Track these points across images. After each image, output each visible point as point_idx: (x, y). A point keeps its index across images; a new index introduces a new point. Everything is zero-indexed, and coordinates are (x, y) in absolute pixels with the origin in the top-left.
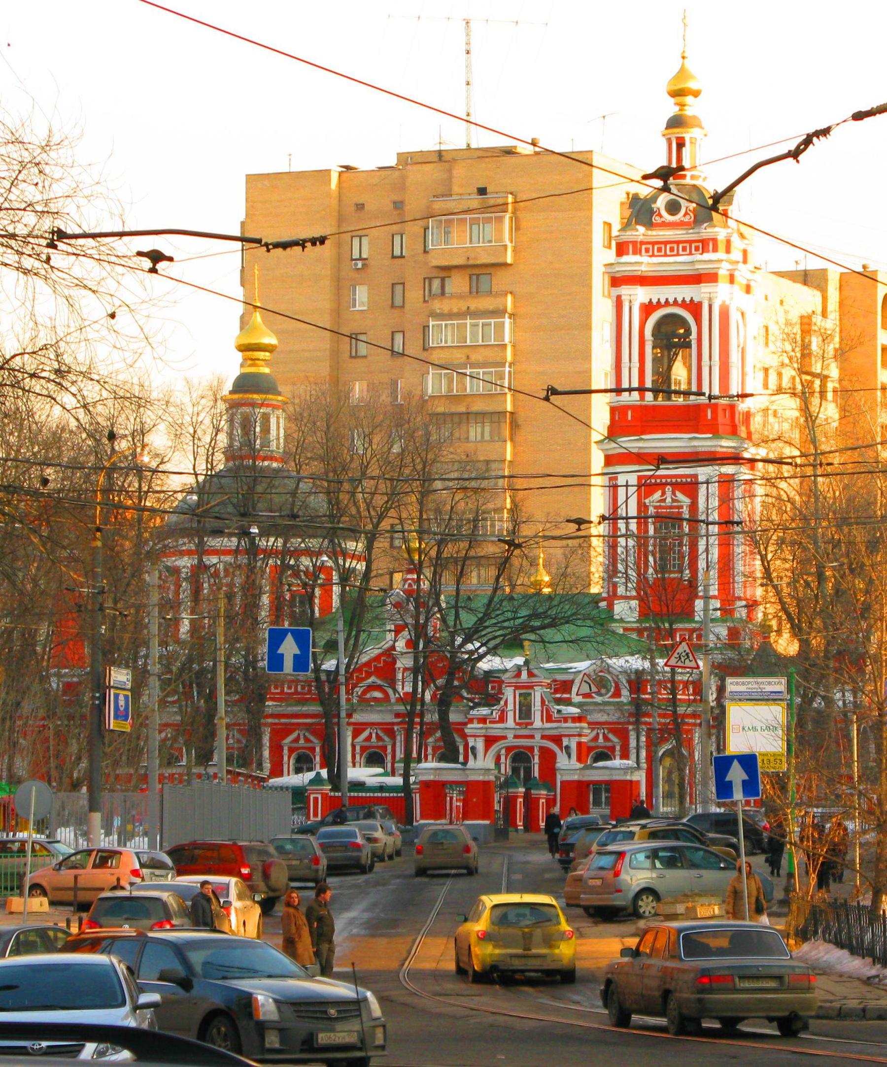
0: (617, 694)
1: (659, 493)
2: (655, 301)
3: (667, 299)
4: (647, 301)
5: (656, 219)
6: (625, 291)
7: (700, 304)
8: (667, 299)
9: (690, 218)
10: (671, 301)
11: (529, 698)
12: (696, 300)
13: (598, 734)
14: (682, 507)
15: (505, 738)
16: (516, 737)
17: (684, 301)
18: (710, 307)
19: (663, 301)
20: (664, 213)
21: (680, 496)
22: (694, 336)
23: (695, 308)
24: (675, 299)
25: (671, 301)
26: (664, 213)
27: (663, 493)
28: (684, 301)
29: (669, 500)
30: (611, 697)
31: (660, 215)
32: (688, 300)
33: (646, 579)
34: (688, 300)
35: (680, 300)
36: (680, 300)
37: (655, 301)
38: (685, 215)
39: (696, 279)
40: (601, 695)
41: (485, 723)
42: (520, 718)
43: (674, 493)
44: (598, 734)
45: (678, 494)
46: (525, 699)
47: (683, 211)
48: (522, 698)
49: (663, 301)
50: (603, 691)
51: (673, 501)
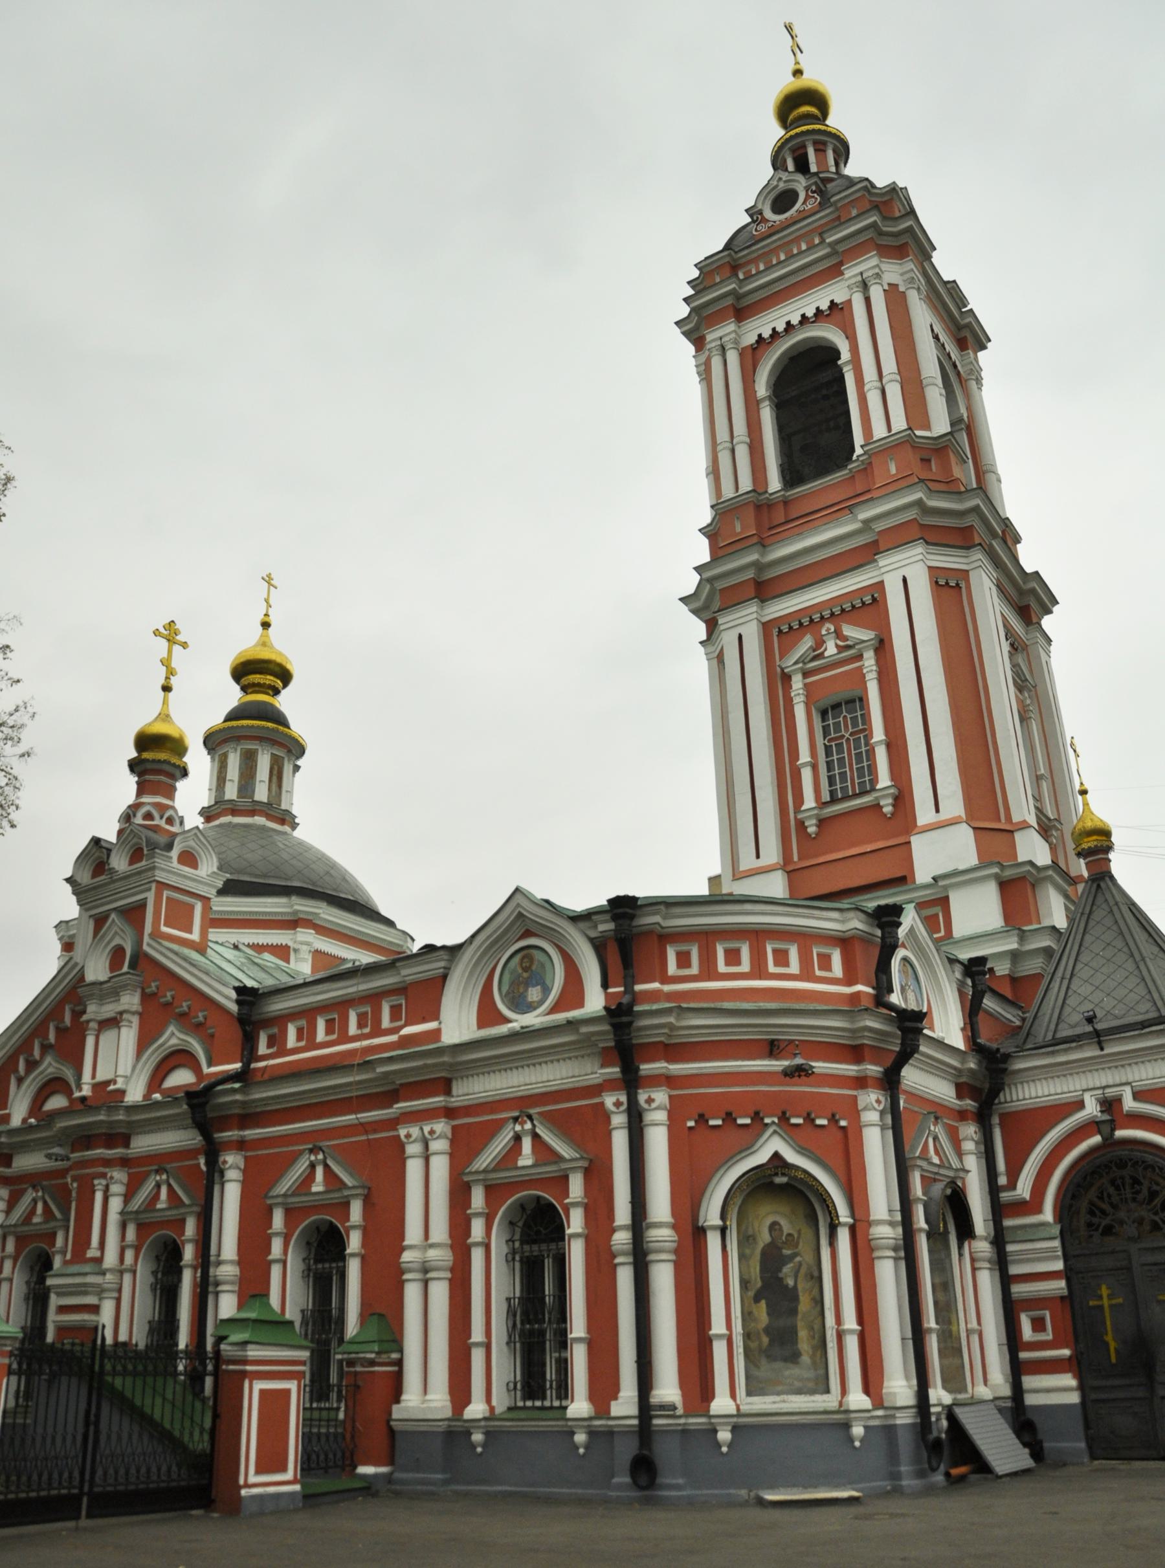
0: (573, 993)
1: (807, 642)
2: (766, 334)
4: (751, 339)
7: (849, 302)
8: (788, 323)
10: (795, 321)
12: (838, 300)
13: (518, 1138)
14: (860, 657)
18: (868, 300)
20: (768, 214)
21: (852, 632)
22: (845, 356)
23: (837, 312)
25: (795, 321)
26: (768, 214)
27: (820, 643)
28: (819, 312)
29: (831, 649)
30: (554, 1010)
31: (765, 220)
32: (824, 306)
33: (801, 825)
35: (810, 313)
36: (810, 313)
38: (804, 203)
39: (834, 272)
40: (530, 1007)
43: (838, 634)
44: (518, 1138)
45: (849, 631)
49: (781, 327)
50: (534, 994)
51: (841, 649)
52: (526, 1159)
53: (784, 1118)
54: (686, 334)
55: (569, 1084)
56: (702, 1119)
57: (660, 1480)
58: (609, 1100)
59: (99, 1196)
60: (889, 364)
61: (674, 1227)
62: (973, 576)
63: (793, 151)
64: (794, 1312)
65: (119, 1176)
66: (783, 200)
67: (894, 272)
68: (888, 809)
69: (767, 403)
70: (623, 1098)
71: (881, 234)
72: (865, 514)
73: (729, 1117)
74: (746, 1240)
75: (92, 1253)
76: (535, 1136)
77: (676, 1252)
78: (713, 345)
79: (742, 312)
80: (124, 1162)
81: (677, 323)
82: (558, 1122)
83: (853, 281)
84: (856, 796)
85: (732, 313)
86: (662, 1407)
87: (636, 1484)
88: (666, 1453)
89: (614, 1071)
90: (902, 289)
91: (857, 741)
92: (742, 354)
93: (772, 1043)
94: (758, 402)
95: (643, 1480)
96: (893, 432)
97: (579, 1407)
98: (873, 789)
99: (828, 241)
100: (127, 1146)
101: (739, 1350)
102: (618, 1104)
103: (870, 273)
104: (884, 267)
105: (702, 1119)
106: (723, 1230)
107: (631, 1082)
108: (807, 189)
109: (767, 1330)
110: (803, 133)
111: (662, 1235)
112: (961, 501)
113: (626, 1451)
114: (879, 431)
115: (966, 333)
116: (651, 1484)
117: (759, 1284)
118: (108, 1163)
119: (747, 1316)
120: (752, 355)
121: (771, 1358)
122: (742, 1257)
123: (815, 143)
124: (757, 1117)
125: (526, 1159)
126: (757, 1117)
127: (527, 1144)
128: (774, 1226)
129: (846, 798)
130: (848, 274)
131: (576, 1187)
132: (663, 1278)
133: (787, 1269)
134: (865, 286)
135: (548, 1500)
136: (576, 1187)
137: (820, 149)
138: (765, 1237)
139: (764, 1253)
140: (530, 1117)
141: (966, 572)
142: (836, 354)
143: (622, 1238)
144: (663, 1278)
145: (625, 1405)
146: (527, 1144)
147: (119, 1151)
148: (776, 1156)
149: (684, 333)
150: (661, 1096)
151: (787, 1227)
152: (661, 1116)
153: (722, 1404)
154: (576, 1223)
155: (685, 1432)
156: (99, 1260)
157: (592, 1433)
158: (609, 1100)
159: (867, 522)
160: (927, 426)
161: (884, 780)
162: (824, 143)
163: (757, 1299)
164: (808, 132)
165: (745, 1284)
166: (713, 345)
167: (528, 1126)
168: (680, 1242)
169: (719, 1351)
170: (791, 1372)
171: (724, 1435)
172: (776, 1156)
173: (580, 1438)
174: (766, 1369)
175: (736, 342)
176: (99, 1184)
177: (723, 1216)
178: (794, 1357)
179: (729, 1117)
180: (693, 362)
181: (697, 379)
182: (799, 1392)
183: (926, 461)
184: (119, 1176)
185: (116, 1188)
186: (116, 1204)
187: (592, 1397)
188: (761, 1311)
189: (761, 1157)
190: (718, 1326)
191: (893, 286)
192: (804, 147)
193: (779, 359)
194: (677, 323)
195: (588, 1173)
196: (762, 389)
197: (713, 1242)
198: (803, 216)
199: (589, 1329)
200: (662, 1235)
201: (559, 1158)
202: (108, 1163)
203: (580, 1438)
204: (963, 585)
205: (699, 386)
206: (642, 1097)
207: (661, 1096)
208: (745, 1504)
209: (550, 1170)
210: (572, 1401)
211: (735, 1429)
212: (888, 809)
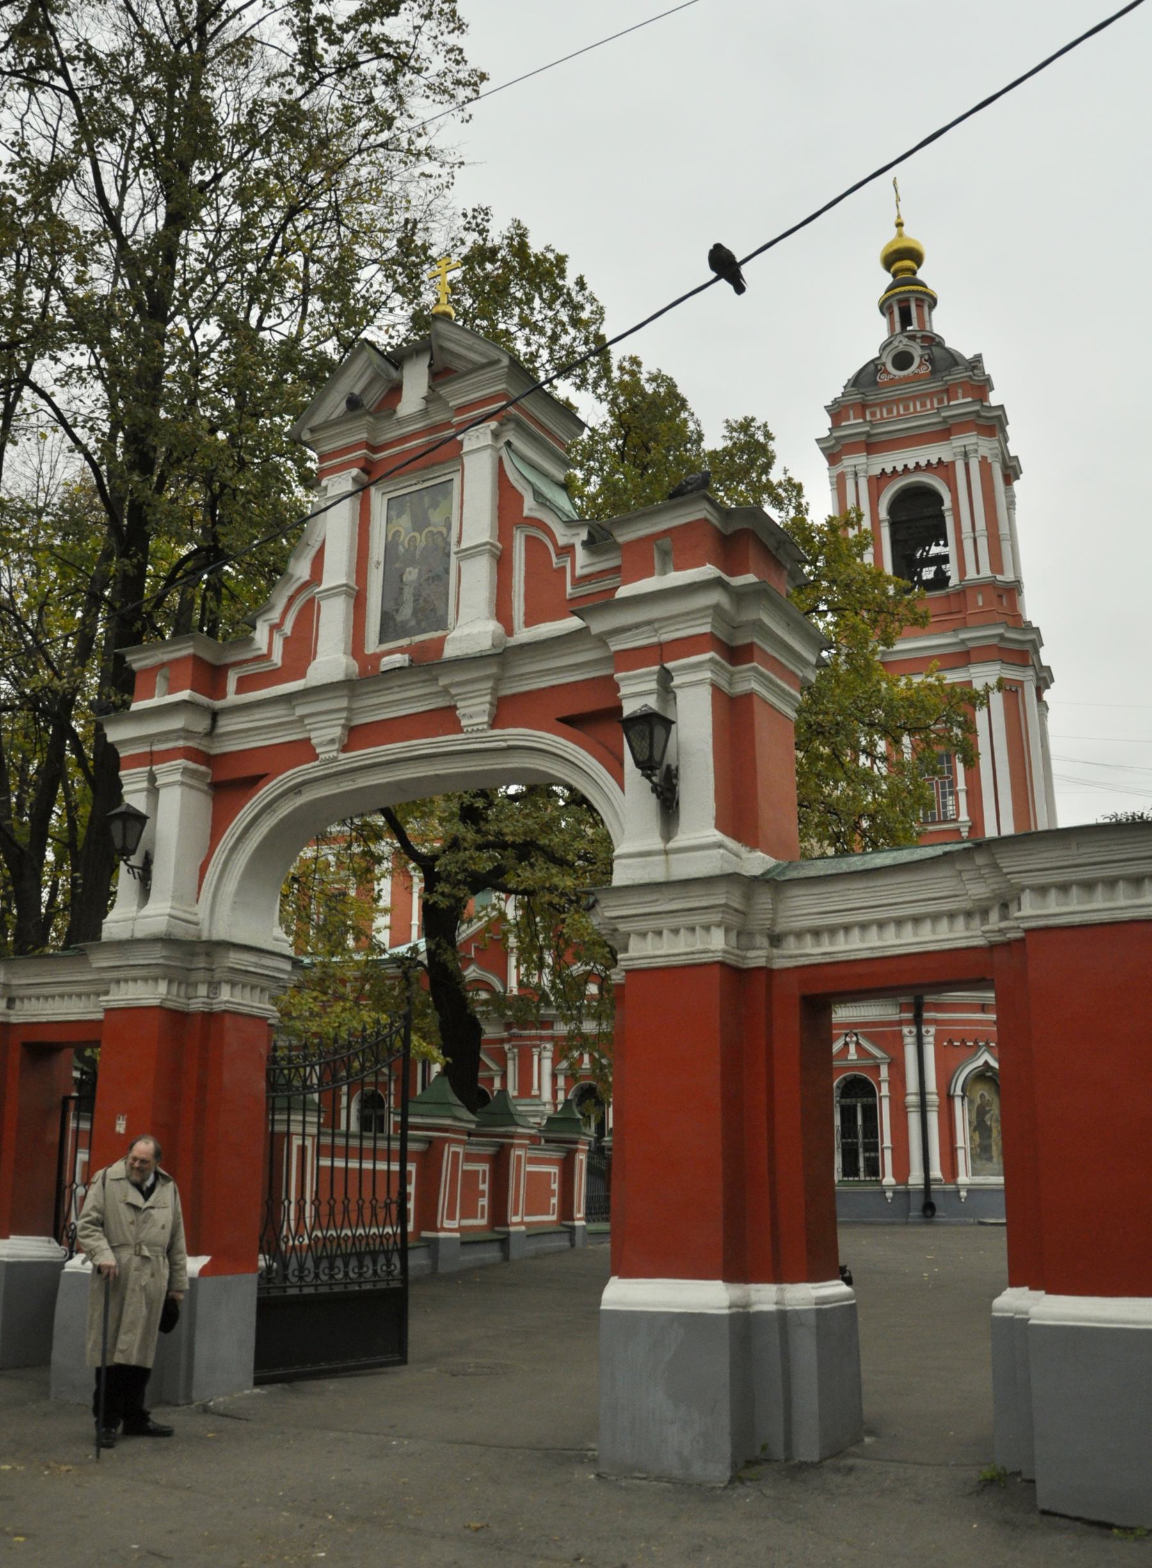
2: (889, 470)
3: (906, 466)
4: (877, 471)
5: (882, 378)
6: (850, 462)
7: (953, 463)
8: (906, 466)
9: (926, 369)
10: (911, 466)
11: (436, 517)
12: (946, 459)
13: (846, 1044)
15: (304, 750)
16: (355, 736)
17: (929, 464)
19: (900, 468)
20: (890, 367)
22: (947, 504)
23: (944, 469)
24: (917, 463)
25: (911, 466)
26: (890, 367)
28: (929, 464)
31: (887, 372)
32: (934, 461)
34: (934, 461)
35: (923, 463)
36: (923, 463)
37: (889, 470)
38: (919, 367)
39: (944, 433)
41: (218, 691)
42: (388, 629)
44: (846, 1044)
46: (420, 523)
47: (917, 361)
48: (404, 523)
49: (900, 468)
52: (853, 1054)
53: (987, 1044)
54: (823, 450)
55: (878, 1019)
56: (950, 1042)
57: (937, 1214)
58: (906, 1030)
59: (536, 1058)
60: (981, 524)
61: (938, 1094)
62: (1025, 684)
63: (899, 301)
64: (990, 1137)
65: (549, 1046)
66: (903, 360)
67: (985, 446)
68: (965, 834)
69: (886, 524)
70: (914, 1030)
71: (979, 416)
72: (963, 636)
73: (963, 1042)
74: (971, 1102)
75: (535, 1092)
76: (857, 1044)
77: (938, 1106)
78: (849, 469)
79: (871, 446)
80: (552, 1038)
81: (817, 440)
82: (874, 1038)
83: (958, 450)
84: (940, 822)
85: (864, 446)
86: (936, 1180)
87: (926, 1216)
88: (936, 1200)
89: (909, 1015)
90: (989, 460)
91: (943, 784)
92: (870, 480)
93: (983, 1005)
94: (880, 522)
95: (929, 1213)
96: (981, 576)
97: (889, 1180)
98: (955, 820)
99: (943, 414)
100: (552, 1028)
101: (969, 1155)
102: (910, 1032)
103: (971, 448)
104: (980, 442)
105: (950, 1042)
106: (963, 1098)
107: (918, 1021)
108: (921, 356)
109: (980, 1145)
110: (909, 292)
111: (933, 1098)
112: (1024, 634)
113: (917, 1202)
114: (971, 574)
115: (1010, 472)
116: (933, 1215)
117: (975, 1123)
118: (541, 1038)
119: (971, 1138)
120: (878, 482)
121: (981, 1159)
122: (969, 1110)
123: (917, 299)
124: (976, 1042)
125: (853, 1054)
126: (976, 1042)
127: (852, 1048)
128: (982, 1096)
129: (933, 823)
130: (956, 443)
131: (884, 1072)
132: (933, 1119)
133: (988, 1117)
134: (966, 455)
135: (871, 1224)
136: (884, 1072)
137: (919, 306)
138: (978, 1101)
139: (978, 1108)
140: (856, 1035)
141: (1022, 682)
142: (940, 500)
143: (912, 1100)
144: (933, 1119)
145: (916, 1178)
146: (852, 1048)
147: (544, 1032)
148: (986, 1063)
149: (822, 449)
150: (932, 1030)
151: (987, 1097)
152: (931, 1039)
153: (963, 1179)
154: (885, 1090)
155: (944, 1192)
156: (539, 1097)
157: (895, 1193)
158: (906, 1030)
159: (963, 641)
160: (1001, 572)
161: (964, 817)
162: (922, 301)
163: (975, 1130)
164: (913, 291)
165: (970, 1123)
166: (849, 469)
167: (855, 1039)
168: (940, 1102)
169: (961, 1154)
170: (989, 1165)
171: (963, 1194)
172: (986, 1063)
173: (889, 1194)
174: (979, 1163)
175: (866, 472)
176: (535, 1051)
177: (963, 1090)
178: (990, 1159)
179: (963, 1042)
180: (827, 473)
181: (829, 487)
182: (993, 1175)
183: (1000, 596)
184: (549, 1046)
185: (548, 1054)
186: (547, 1065)
187: (894, 1176)
188: (977, 1136)
189: (980, 1062)
190: (960, 1143)
191: (984, 458)
192: (907, 300)
193: (896, 492)
194: (817, 440)
195: (890, 1065)
196: (883, 514)
197: (958, 1102)
198: (916, 377)
199: (892, 1141)
200: (933, 1098)
201: (875, 1058)
202: (541, 1038)
203: (889, 1194)
204: (1020, 691)
205: (830, 493)
206: (924, 1029)
207: (932, 1030)
208: (973, 1224)
209: (870, 1062)
210: (884, 1176)
211: (968, 1191)
212: (965, 834)
